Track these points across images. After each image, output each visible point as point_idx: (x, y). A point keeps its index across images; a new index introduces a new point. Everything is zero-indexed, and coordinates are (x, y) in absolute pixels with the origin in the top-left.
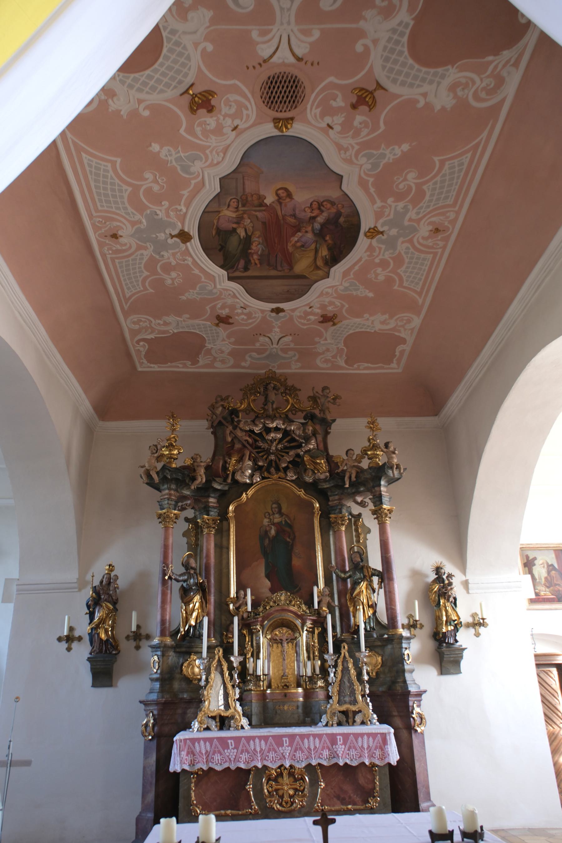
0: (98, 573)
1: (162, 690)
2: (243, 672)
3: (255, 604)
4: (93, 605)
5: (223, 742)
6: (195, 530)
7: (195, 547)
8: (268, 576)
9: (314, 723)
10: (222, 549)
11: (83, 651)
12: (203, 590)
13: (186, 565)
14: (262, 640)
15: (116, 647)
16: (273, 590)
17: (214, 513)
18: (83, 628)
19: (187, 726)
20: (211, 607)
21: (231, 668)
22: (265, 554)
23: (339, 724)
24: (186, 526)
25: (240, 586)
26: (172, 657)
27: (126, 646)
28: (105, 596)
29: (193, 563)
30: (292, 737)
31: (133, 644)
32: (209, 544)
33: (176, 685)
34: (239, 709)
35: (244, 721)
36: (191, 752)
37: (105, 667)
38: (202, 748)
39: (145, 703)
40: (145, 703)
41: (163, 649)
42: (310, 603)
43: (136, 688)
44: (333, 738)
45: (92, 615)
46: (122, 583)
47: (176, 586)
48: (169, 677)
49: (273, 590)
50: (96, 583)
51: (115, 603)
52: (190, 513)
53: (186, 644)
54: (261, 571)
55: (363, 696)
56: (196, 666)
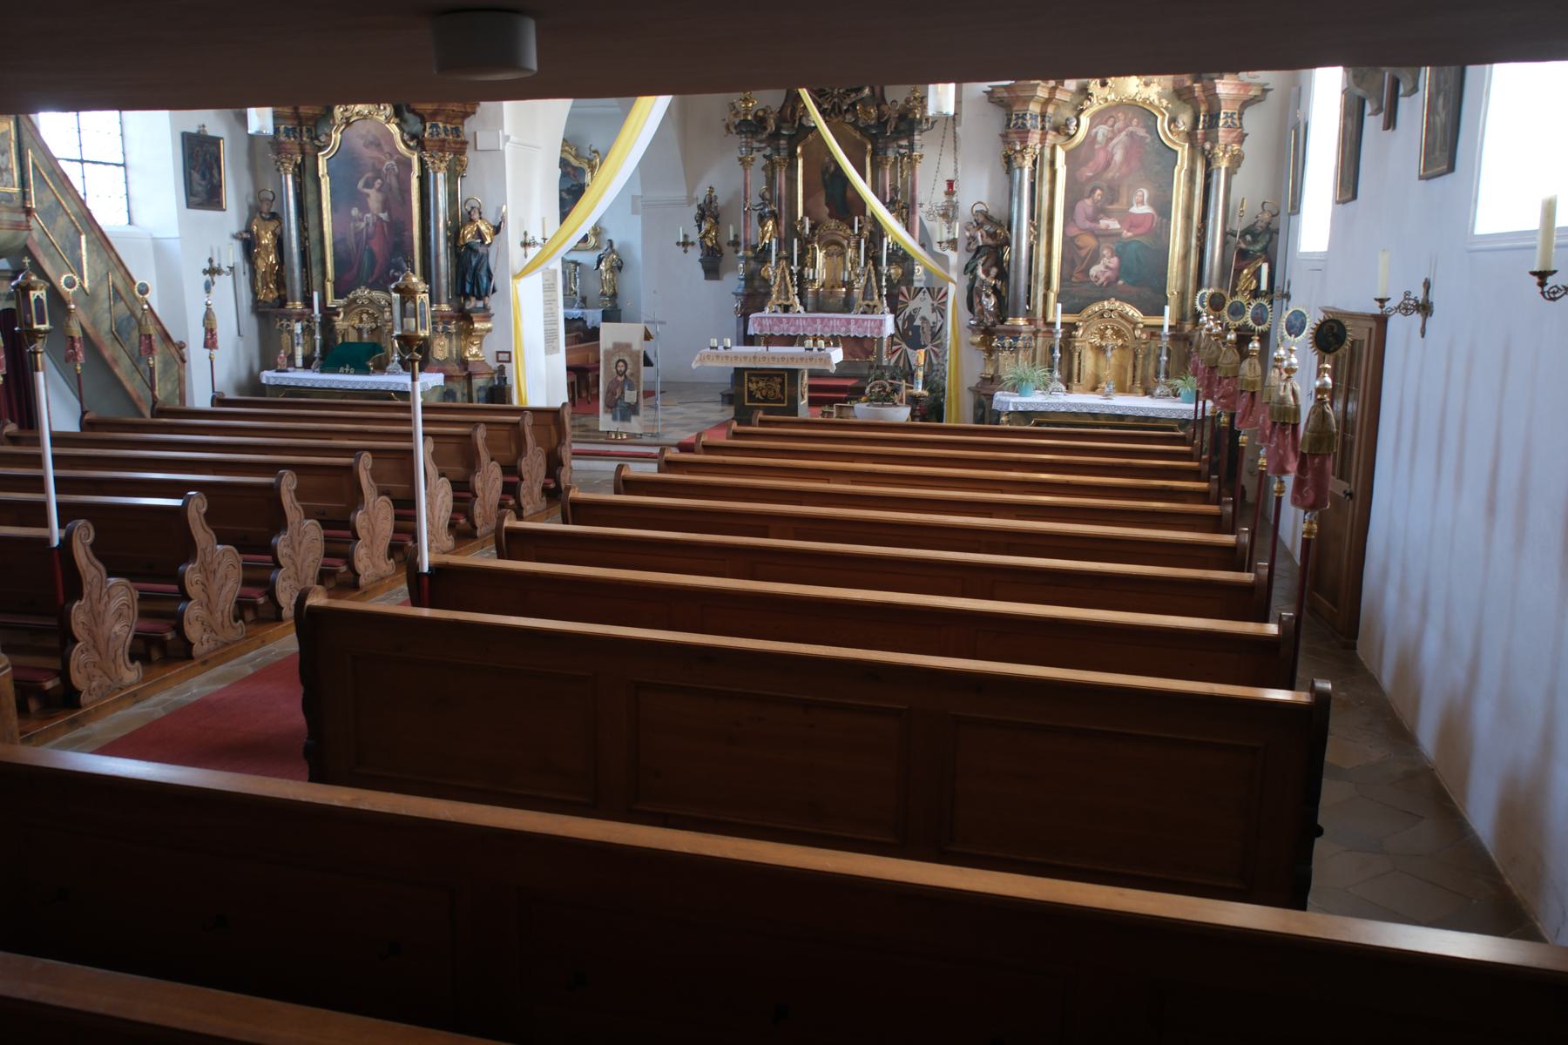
0: (701, 194)
1: (746, 287)
2: (800, 274)
3: (813, 228)
4: (701, 218)
5: (780, 319)
6: (770, 169)
7: (771, 182)
8: (827, 204)
9: (849, 311)
10: (792, 181)
11: (696, 253)
12: (775, 217)
13: (762, 196)
14: (820, 255)
15: (720, 251)
16: (831, 216)
17: (784, 154)
18: (695, 236)
19: (762, 310)
20: (782, 229)
21: (791, 274)
22: (826, 186)
23: (864, 313)
24: (764, 162)
25: (806, 213)
26: (753, 264)
27: (728, 250)
28: (708, 212)
29: (767, 196)
30: (822, 319)
31: (732, 249)
32: (781, 179)
33: (757, 283)
34: (797, 300)
35: (801, 308)
36: (760, 324)
37: (713, 265)
38: (767, 322)
39: (736, 294)
40: (736, 294)
41: (746, 259)
42: (852, 228)
43: (733, 282)
44: (848, 321)
45: (700, 227)
46: (721, 202)
47: (755, 215)
48: (750, 278)
49: (831, 216)
50: (701, 201)
51: (716, 218)
52: (768, 151)
53: (762, 255)
54: (822, 200)
55: (880, 295)
56: (771, 271)
